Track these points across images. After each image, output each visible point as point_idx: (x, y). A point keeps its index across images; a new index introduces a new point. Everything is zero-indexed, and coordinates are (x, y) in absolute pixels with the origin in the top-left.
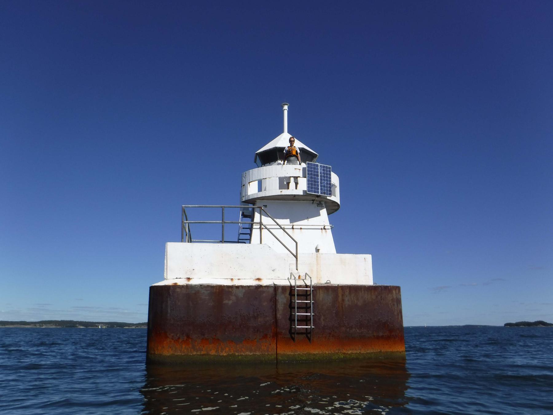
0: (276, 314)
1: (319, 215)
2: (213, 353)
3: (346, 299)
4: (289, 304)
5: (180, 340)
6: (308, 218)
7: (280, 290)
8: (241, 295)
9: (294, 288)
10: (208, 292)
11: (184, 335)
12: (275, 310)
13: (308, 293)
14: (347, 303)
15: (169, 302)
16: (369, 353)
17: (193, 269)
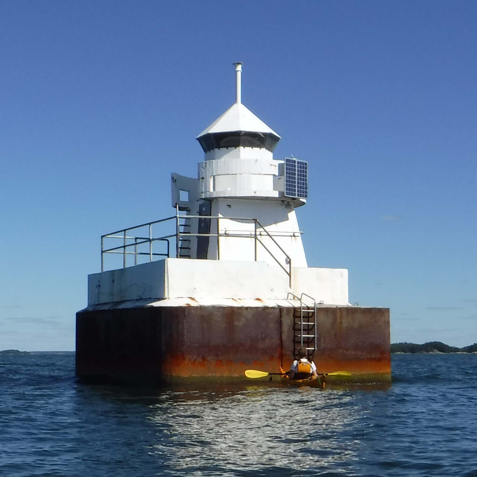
0: (281, 337)
1: (287, 219)
2: (226, 374)
3: (344, 321)
4: (292, 326)
5: (197, 362)
6: (276, 222)
7: (284, 312)
8: (250, 317)
9: (300, 310)
10: (221, 313)
11: (200, 357)
12: (281, 333)
13: (310, 315)
14: (345, 325)
15: (185, 324)
16: (363, 375)
17: (195, 288)
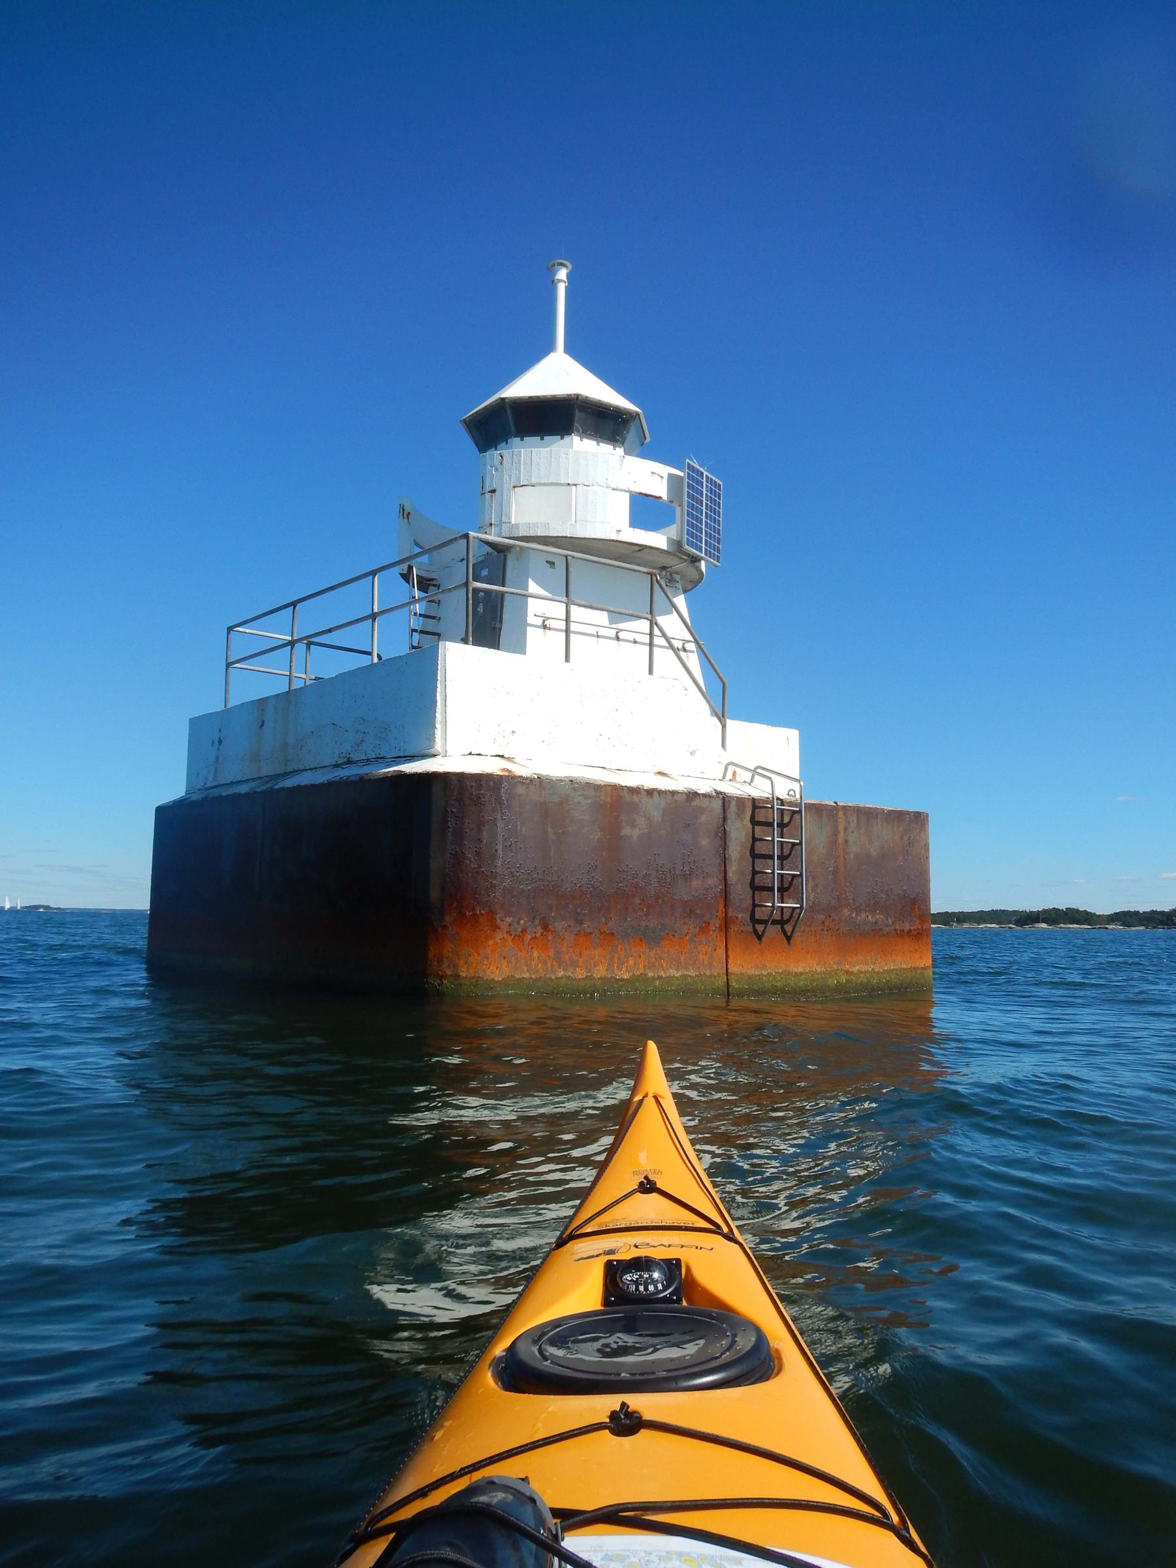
2: (600, 972)
7: (732, 809)
8: (657, 815)
11: (537, 922)
12: (725, 860)
14: (853, 849)
15: (500, 824)
